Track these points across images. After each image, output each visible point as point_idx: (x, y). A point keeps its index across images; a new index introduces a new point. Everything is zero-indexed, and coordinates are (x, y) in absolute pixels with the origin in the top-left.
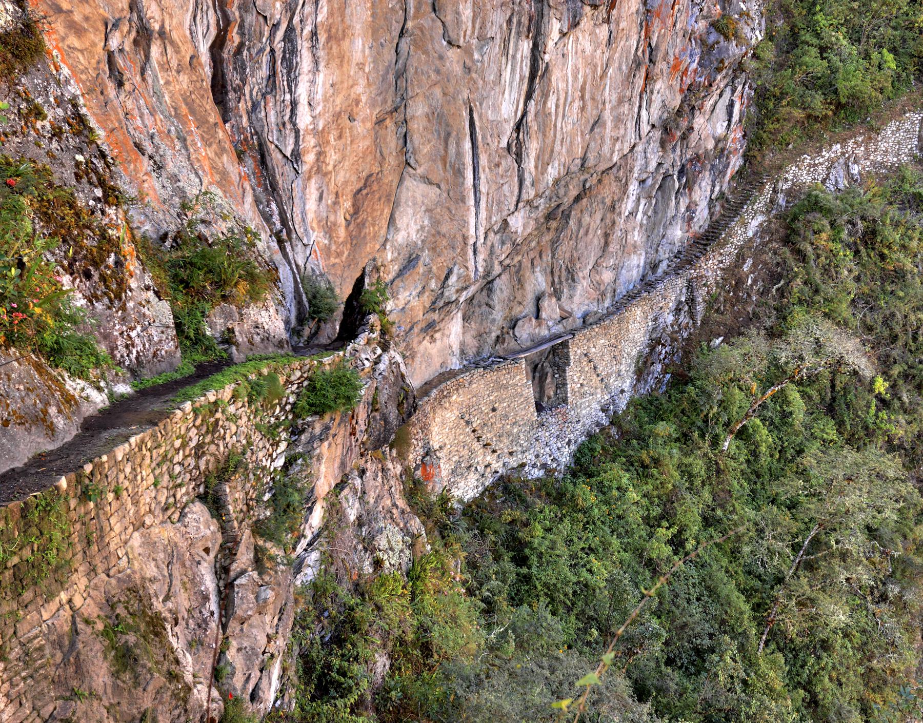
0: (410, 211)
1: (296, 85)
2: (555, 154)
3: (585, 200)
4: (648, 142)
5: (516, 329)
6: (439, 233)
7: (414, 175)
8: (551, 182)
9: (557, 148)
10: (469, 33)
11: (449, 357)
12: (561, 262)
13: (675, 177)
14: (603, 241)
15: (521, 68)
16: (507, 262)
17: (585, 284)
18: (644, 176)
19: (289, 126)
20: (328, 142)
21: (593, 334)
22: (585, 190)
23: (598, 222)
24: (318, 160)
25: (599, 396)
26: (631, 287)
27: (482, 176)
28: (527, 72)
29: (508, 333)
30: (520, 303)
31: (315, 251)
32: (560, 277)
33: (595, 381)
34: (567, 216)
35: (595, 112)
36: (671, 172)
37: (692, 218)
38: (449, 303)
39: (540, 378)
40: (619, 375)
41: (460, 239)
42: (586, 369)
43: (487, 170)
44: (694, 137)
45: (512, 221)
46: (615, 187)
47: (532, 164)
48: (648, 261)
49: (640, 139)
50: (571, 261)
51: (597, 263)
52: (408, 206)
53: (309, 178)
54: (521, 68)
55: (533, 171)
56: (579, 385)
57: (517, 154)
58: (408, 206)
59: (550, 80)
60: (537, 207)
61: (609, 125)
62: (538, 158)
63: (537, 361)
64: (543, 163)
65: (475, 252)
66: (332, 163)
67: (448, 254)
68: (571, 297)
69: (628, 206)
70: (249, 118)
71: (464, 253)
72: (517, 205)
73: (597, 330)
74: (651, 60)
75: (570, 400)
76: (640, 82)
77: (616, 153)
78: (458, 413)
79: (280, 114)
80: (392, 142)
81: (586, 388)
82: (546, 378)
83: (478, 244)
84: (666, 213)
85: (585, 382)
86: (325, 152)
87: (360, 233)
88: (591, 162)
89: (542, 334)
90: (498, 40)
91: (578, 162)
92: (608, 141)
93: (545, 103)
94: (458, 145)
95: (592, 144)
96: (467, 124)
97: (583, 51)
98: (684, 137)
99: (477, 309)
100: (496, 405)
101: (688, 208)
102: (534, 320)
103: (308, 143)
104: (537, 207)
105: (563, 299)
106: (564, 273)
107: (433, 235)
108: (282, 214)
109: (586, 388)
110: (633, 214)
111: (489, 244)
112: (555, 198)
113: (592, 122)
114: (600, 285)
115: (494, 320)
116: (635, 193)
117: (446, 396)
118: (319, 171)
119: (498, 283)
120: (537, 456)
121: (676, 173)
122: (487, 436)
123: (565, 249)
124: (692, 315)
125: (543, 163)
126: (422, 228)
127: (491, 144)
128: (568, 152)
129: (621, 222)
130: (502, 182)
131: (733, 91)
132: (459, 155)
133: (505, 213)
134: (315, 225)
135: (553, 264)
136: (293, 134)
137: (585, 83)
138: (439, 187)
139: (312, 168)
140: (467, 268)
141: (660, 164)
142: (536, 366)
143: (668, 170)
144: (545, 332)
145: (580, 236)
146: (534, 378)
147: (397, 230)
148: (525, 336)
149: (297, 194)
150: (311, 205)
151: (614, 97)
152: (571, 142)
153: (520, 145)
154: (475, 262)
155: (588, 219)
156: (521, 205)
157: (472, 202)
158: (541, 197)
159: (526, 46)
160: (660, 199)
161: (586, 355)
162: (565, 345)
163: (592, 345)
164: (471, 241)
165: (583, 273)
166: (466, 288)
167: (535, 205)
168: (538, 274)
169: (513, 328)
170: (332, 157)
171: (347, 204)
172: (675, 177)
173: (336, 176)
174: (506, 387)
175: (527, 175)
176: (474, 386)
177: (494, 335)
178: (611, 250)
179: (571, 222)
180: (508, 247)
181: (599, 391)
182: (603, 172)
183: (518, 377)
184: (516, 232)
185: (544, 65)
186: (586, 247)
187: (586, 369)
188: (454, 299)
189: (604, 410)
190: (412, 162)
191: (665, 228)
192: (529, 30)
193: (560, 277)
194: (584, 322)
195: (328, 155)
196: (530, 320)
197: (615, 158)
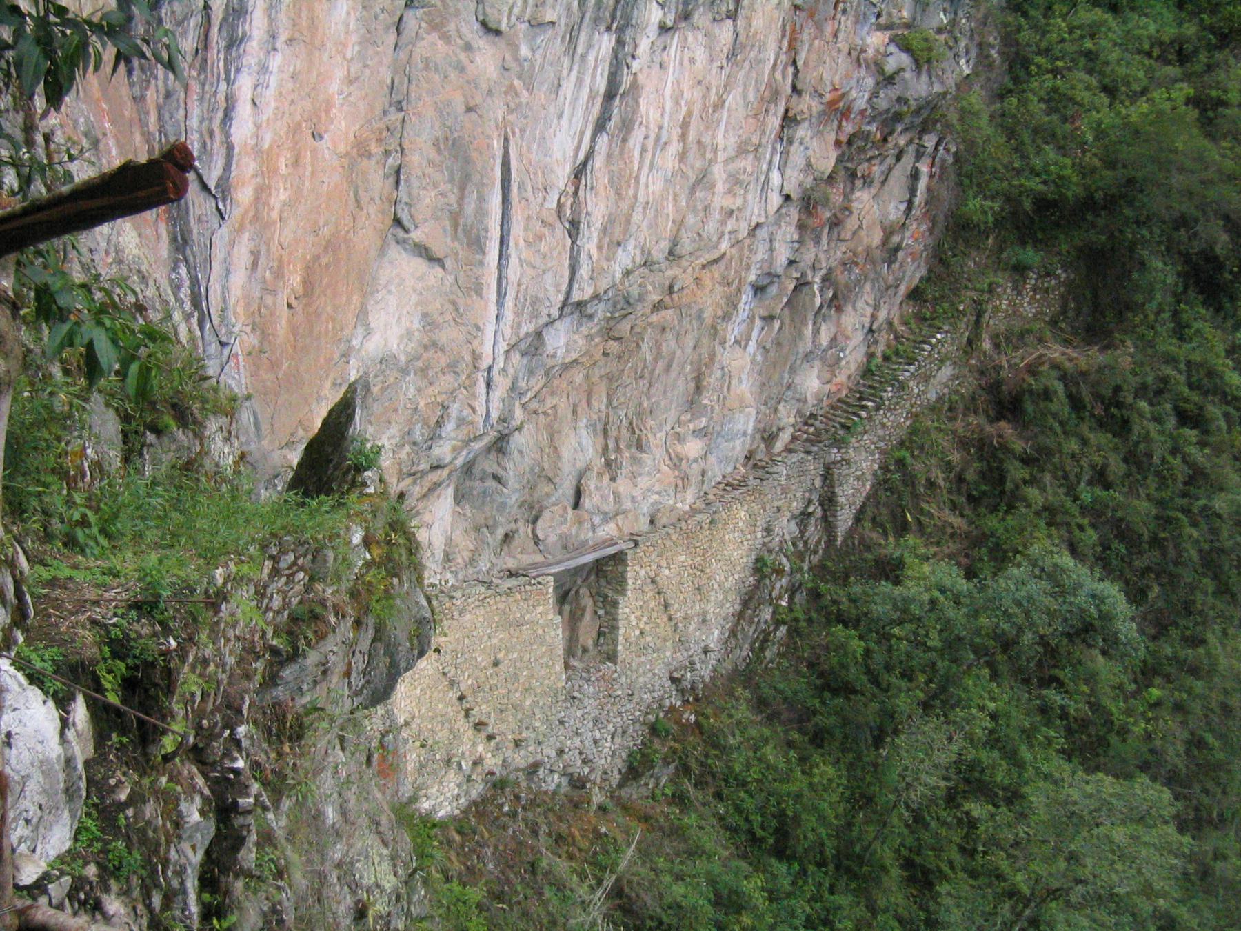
0: (393, 301)
1: (238, 71)
2: (633, 229)
5: (540, 524)
6: (434, 344)
7: (404, 241)
8: (618, 276)
9: (637, 217)
10: (516, 11)
14: (692, 385)
15: (593, 76)
16: (534, 405)
19: (218, 136)
20: (276, 170)
21: (668, 543)
23: (689, 350)
24: (257, 199)
27: (512, 251)
28: (602, 85)
30: (550, 480)
31: (236, 356)
32: (617, 440)
33: (664, 628)
35: (698, 164)
36: (809, 278)
37: (840, 359)
39: (572, 615)
40: (704, 621)
41: (468, 358)
42: (652, 604)
43: (522, 243)
44: (851, 224)
45: (548, 335)
47: (595, 240)
52: (390, 292)
53: (240, 229)
54: (593, 76)
55: (594, 252)
58: (390, 292)
59: (637, 103)
60: (591, 317)
61: (720, 187)
62: (604, 230)
63: (566, 587)
65: (489, 384)
66: (278, 206)
67: (447, 381)
68: (634, 476)
70: (160, 117)
71: (470, 386)
72: (562, 309)
74: (794, 88)
75: (620, 658)
76: (774, 122)
79: (206, 118)
80: (378, 182)
83: (495, 371)
85: (648, 627)
86: (269, 187)
87: (311, 332)
88: (686, 245)
90: (562, 27)
91: (665, 245)
92: (717, 216)
93: (624, 140)
94: (482, 199)
95: (691, 220)
96: (499, 161)
97: (692, 61)
98: (835, 223)
99: (477, 484)
100: (501, 655)
101: (834, 340)
102: (570, 510)
103: (246, 168)
104: (591, 317)
105: (619, 481)
106: (625, 433)
107: (426, 348)
108: (195, 282)
109: (648, 639)
111: (511, 371)
113: (693, 179)
118: (256, 218)
119: (518, 440)
120: (560, 752)
121: (817, 280)
122: (481, 710)
124: (828, 525)
126: (409, 334)
128: (650, 227)
131: (919, 156)
132: (481, 212)
134: (240, 310)
135: (608, 415)
136: (223, 151)
137: (689, 114)
138: (443, 267)
139: (246, 212)
140: (474, 410)
141: (791, 263)
142: (567, 593)
143: (803, 274)
144: (586, 535)
147: (368, 332)
148: (553, 538)
149: (218, 255)
150: (238, 279)
151: (732, 141)
154: (487, 401)
155: (673, 344)
156: (567, 310)
157: (493, 297)
159: (606, 42)
160: (787, 321)
163: (664, 563)
164: (484, 365)
165: (656, 440)
168: (584, 432)
169: (535, 520)
170: (280, 195)
171: (295, 280)
173: (281, 230)
175: (583, 258)
176: (468, 617)
177: (500, 532)
178: (706, 401)
179: (645, 347)
180: (538, 382)
181: (669, 644)
182: (704, 267)
184: (554, 356)
185: (631, 77)
186: (665, 392)
190: (404, 217)
192: (613, 18)
193: (617, 440)
194: (652, 522)
195: (274, 192)
196: (565, 509)
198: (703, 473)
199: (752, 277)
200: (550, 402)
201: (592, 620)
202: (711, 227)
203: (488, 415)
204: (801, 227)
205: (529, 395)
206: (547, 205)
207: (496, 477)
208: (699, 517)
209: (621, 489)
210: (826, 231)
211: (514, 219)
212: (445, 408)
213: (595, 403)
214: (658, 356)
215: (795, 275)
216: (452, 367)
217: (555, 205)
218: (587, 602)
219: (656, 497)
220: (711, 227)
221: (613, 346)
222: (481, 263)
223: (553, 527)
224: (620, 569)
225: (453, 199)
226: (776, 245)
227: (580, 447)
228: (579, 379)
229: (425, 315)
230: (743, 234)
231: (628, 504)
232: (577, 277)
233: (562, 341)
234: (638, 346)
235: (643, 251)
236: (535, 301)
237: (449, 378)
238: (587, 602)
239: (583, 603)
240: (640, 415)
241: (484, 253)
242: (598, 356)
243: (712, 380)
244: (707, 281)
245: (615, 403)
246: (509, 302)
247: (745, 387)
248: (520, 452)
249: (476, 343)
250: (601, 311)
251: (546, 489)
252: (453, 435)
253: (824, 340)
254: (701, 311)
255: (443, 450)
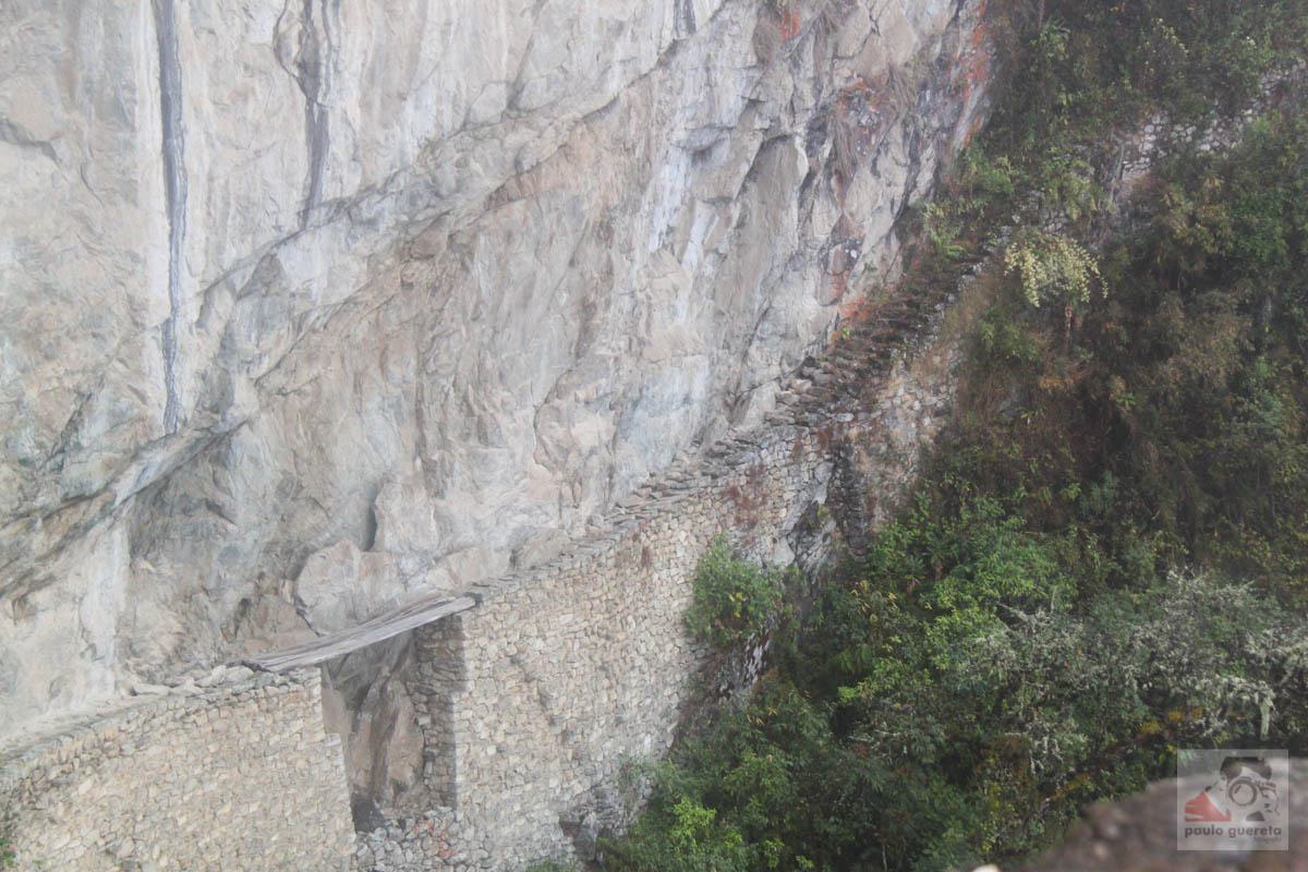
3: (518, 206)
4: (716, 38)
5: (302, 578)
6: (47, 289)
8: (412, 151)
9: (430, 49)
11: (78, 662)
12: (447, 384)
13: (798, 141)
14: (574, 325)
16: (278, 380)
17: (519, 450)
18: (706, 139)
21: (538, 595)
22: (519, 174)
23: (561, 267)
25: (553, 783)
26: (664, 460)
29: (276, 591)
30: (316, 503)
33: (542, 737)
34: (463, 251)
36: (786, 128)
38: (81, 498)
40: (619, 721)
41: (121, 310)
42: (517, 701)
43: (208, 107)
46: (612, 167)
48: (719, 385)
49: (691, 28)
50: (479, 384)
51: (558, 391)
55: (355, 114)
56: (492, 751)
57: (302, 66)
63: (365, 679)
64: (389, 89)
65: (168, 351)
68: (476, 487)
69: (645, 232)
71: (130, 352)
72: (304, 214)
73: (549, 585)
75: (462, 796)
77: (617, 69)
78: (94, 835)
81: (514, 760)
82: (392, 727)
83: (180, 327)
84: (772, 245)
85: (511, 741)
88: (537, 93)
89: (383, 595)
91: (500, 93)
94: (112, 32)
95: (543, 44)
99: (179, 520)
101: (840, 231)
102: (357, 554)
104: (371, 223)
105: (448, 495)
107: (31, 297)
109: (514, 760)
110: (674, 240)
111: (216, 326)
112: (427, 198)
114: (567, 452)
115: (231, 553)
116: (679, 185)
117: (55, 785)
121: (801, 129)
123: (459, 347)
125: (389, 89)
127: (220, 29)
129: (631, 272)
130: (255, 145)
132: (117, 59)
133: (267, 237)
135: (420, 388)
138: (52, 155)
140: (143, 398)
141: (753, 104)
142: (363, 692)
143: (776, 120)
144: (390, 591)
145: (505, 308)
146: (355, 727)
152: (475, 34)
153: (308, 35)
154: (169, 380)
156: (318, 215)
157: (160, 202)
158: (383, 193)
160: (754, 204)
161: (514, 661)
162: (448, 626)
163: (532, 630)
164: (155, 316)
165: (515, 423)
166: (135, 456)
167: (366, 215)
168: (378, 419)
169: (295, 575)
172: (798, 141)
174: (258, 755)
175: (334, 125)
176: (153, 751)
177: (232, 598)
178: (602, 351)
179: (478, 269)
180: (279, 340)
181: (554, 766)
183: (299, 724)
184: (306, 295)
186: (524, 342)
187: (517, 701)
188: (97, 485)
189: (567, 827)
191: (770, 290)
194: (514, 561)
196: (346, 552)
197: (615, 84)
198: (611, 471)
199: (680, 135)
200: (306, 374)
201: (410, 731)
202: (584, 56)
203: (171, 396)
204: (761, 41)
205: (267, 364)
206: (254, 38)
207: (213, 507)
208: (600, 547)
209: (454, 509)
210: (809, 46)
211: (187, 66)
212: (85, 398)
213: (394, 369)
214: (504, 282)
215: (758, 124)
216: (93, 327)
217: (268, 37)
218: (403, 706)
219: (522, 518)
220: (584, 56)
221: (421, 272)
222: (129, 146)
223: (330, 583)
224: (452, 645)
225: (57, 36)
226: (717, 76)
227: (370, 441)
228: (361, 330)
229: (23, 242)
230: (647, 62)
231: (468, 534)
232: (328, 158)
233: (320, 267)
234: (464, 267)
235: (455, 105)
236: (246, 206)
237: (88, 345)
238: (403, 706)
239: (392, 707)
240: (479, 384)
241: (133, 129)
242: (393, 288)
243: (612, 317)
244: (585, 148)
245: (432, 367)
246: (194, 210)
247: (683, 320)
248: (254, 461)
249: (132, 283)
250: (388, 211)
251: (311, 520)
252: (105, 442)
253: (821, 229)
254: (576, 200)
255: (86, 470)
